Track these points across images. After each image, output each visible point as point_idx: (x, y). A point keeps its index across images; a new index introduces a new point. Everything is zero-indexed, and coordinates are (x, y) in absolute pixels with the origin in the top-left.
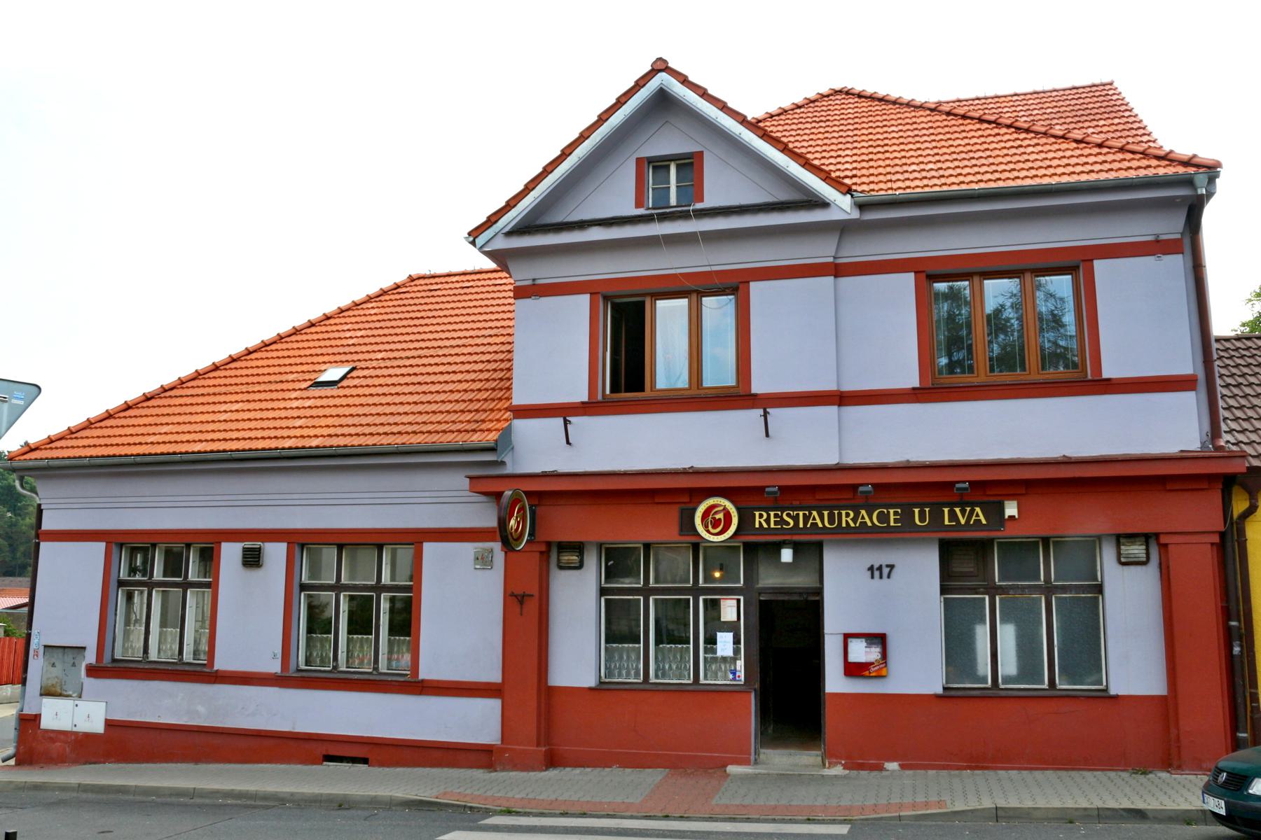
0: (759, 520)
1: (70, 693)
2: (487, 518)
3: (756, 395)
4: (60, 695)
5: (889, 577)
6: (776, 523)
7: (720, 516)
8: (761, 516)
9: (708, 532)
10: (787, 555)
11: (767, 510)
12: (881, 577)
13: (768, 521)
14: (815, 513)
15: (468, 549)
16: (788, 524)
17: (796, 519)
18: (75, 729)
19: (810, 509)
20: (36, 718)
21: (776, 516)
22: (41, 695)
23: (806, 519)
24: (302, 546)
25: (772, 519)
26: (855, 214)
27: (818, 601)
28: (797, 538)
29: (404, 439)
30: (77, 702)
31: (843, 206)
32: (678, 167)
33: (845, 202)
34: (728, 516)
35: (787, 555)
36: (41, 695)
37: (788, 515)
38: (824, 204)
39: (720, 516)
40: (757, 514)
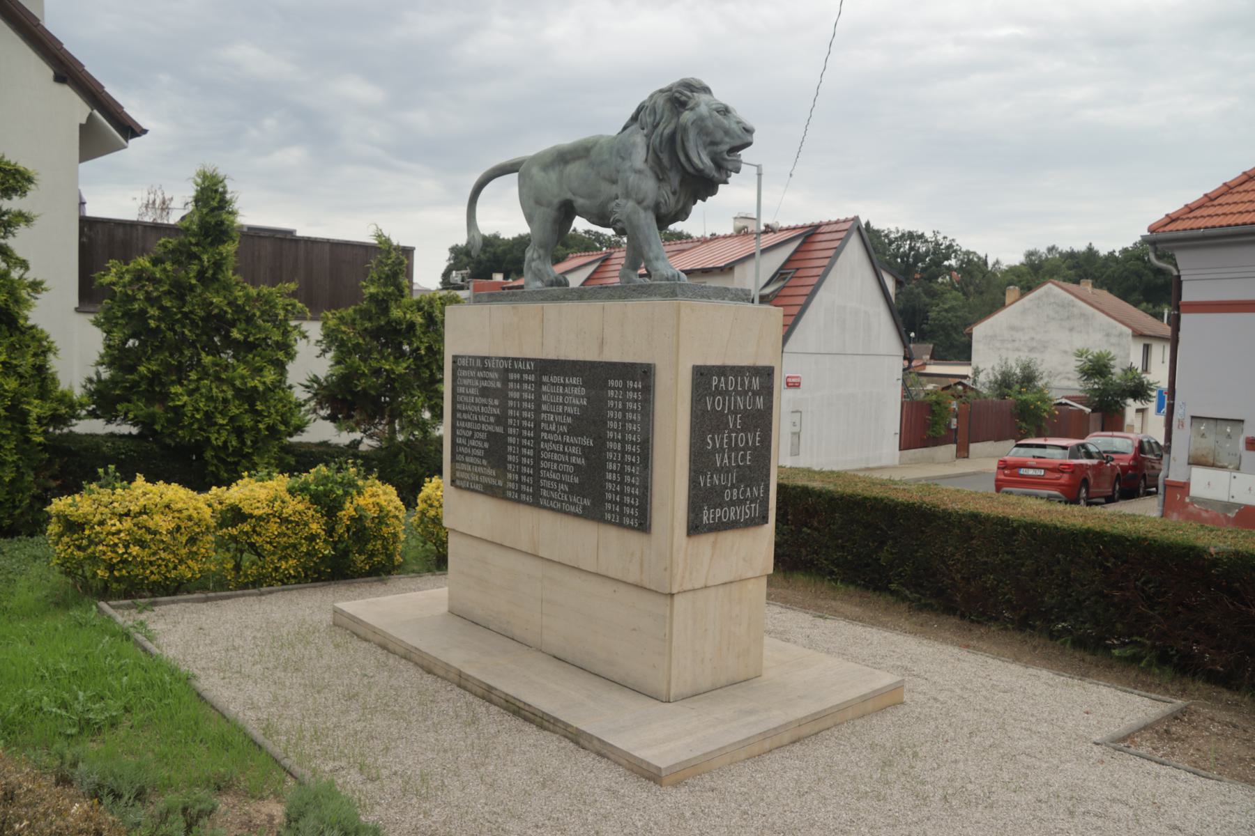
1: (1226, 464)
4: (1213, 466)
18: (1232, 500)
20: (1184, 487)
22: (1189, 464)
30: (1234, 474)
36: (1189, 464)
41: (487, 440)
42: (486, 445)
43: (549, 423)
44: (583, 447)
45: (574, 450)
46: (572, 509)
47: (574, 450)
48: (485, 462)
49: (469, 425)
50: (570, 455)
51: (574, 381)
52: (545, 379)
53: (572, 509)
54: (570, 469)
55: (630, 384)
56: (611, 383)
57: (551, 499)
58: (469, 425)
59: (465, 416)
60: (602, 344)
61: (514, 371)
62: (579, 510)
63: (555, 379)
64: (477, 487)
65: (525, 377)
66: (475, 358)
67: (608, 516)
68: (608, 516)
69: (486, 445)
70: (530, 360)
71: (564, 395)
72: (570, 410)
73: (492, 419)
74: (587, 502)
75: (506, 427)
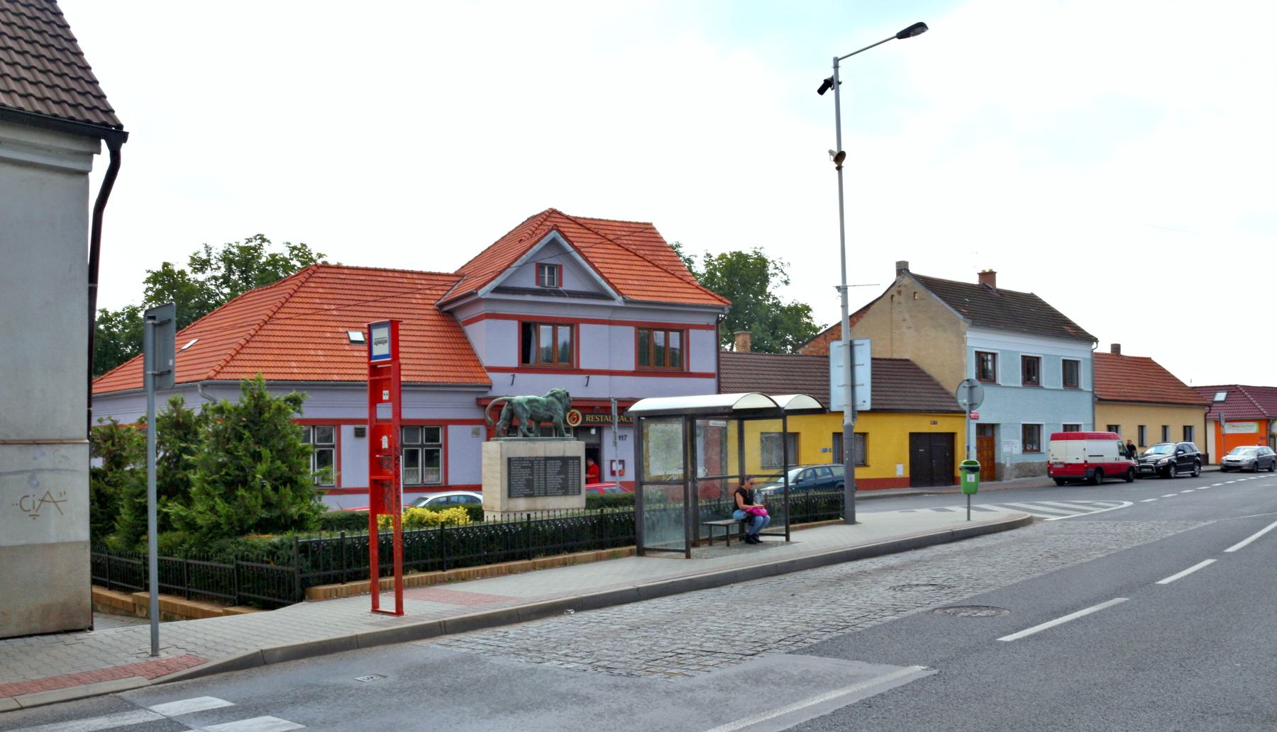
0: (588, 418)
2: (475, 414)
10: (593, 432)
11: (590, 414)
15: (468, 429)
24: (314, 427)
26: (623, 305)
31: (619, 301)
33: (620, 298)
34: (578, 417)
35: (593, 432)
38: (612, 299)
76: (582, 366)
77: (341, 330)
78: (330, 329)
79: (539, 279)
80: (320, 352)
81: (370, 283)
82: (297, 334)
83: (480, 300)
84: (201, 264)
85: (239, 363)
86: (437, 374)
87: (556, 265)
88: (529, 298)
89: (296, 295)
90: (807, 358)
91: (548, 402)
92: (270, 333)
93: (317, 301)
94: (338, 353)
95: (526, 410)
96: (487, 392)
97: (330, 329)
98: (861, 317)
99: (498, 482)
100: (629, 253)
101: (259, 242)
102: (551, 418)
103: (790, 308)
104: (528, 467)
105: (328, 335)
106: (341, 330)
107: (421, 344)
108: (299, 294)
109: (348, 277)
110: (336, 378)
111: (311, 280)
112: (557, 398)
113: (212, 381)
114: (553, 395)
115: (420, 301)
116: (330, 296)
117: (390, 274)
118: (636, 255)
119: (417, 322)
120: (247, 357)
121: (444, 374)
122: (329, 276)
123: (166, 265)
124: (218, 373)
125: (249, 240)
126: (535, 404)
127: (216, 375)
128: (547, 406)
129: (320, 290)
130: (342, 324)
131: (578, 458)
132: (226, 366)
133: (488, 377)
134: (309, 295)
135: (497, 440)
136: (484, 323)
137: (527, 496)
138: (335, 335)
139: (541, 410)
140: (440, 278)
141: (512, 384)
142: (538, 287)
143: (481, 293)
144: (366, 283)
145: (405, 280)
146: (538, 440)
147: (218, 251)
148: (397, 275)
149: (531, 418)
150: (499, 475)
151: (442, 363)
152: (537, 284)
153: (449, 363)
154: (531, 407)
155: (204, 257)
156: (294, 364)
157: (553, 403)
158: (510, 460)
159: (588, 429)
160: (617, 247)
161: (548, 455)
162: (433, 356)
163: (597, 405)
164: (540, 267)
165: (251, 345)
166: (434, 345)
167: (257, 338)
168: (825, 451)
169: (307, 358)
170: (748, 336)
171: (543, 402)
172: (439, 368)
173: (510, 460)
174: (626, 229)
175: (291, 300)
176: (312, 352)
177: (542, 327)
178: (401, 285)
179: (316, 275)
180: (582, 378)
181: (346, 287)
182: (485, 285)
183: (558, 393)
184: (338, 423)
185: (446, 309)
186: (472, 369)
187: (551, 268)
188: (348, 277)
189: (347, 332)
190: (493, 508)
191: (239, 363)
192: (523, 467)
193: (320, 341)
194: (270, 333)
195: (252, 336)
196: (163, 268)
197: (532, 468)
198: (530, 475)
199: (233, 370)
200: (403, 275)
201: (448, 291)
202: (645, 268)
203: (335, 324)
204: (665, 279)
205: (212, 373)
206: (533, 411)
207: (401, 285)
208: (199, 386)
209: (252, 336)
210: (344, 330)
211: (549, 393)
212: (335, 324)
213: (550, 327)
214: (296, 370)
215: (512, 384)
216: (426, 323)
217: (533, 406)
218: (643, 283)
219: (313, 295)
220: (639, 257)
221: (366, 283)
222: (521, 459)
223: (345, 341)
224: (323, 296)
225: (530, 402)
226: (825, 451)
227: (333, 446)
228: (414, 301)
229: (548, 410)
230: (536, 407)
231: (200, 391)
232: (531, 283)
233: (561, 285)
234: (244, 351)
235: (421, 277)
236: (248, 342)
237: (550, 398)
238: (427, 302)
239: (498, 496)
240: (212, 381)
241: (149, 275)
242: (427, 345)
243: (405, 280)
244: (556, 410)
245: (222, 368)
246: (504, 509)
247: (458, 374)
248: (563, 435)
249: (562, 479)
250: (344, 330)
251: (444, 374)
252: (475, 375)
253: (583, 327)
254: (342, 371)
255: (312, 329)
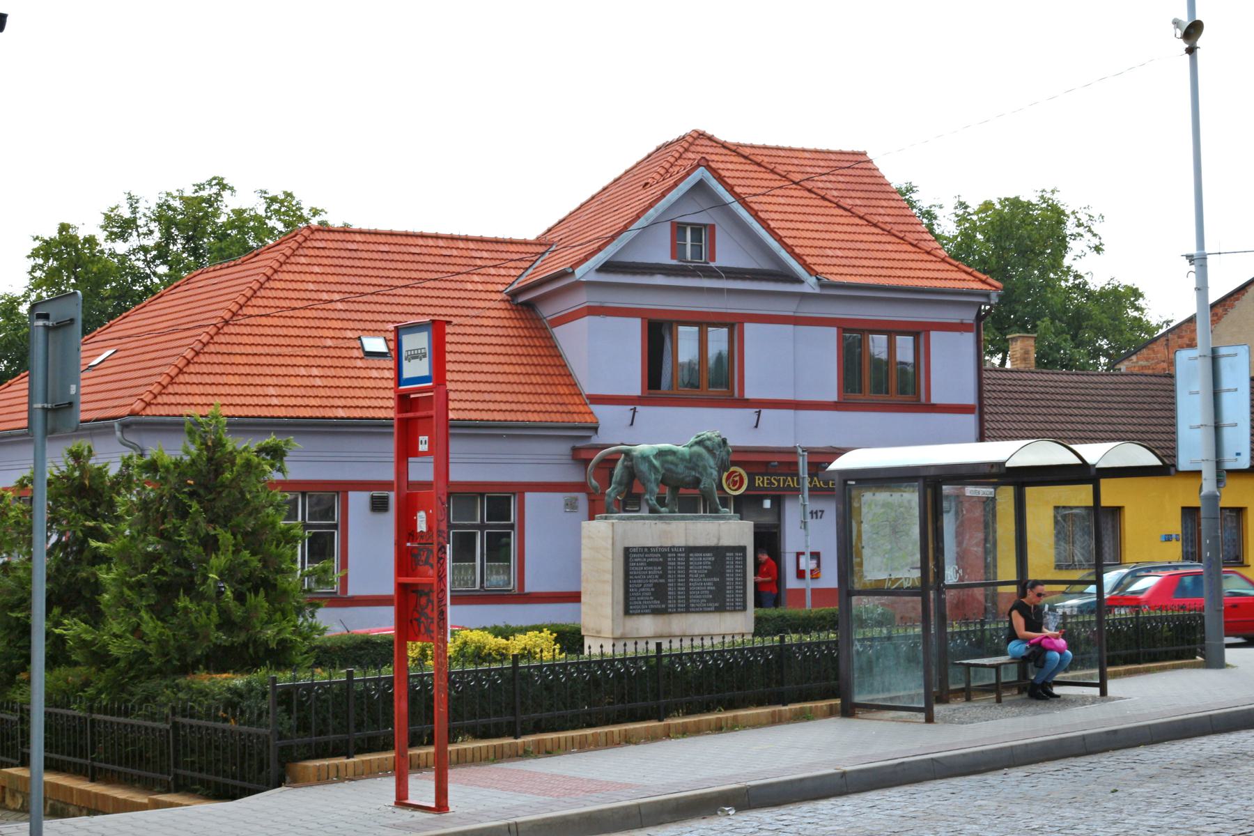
0: (758, 482)
2: (572, 475)
3: (748, 399)
5: (821, 517)
6: (767, 484)
7: (737, 478)
8: (759, 479)
9: (730, 488)
10: (767, 504)
11: (763, 475)
12: (817, 518)
13: (763, 482)
14: (789, 478)
15: (559, 498)
16: (774, 484)
17: (779, 481)
19: (787, 475)
21: (768, 479)
23: (784, 481)
24: (304, 494)
25: (765, 481)
26: (817, 290)
27: (776, 533)
28: (773, 493)
29: (520, 417)
32: (692, 229)
33: (812, 280)
35: (767, 504)
37: (775, 479)
38: (799, 281)
39: (737, 478)
40: (757, 477)
41: (654, 587)
42: (653, 589)
43: (694, 574)
44: (714, 582)
45: (709, 584)
46: (709, 609)
47: (709, 584)
48: (652, 598)
49: (640, 581)
50: (707, 586)
51: (708, 555)
52: (691, 555)
53: (709, 609)
54: (708, 592)
55: (737, 554)
56: (728, 554)
57: (697, 607)
58: (640, 581)
59: (636, 577)
60: (719, 539)
61: (671, 552)
62: (713, 609)
63: (697, 555)
64: (647, 611)
65: (679, 555)
66: (644, 548)
67: (728, 608)
68: (728, 608)
69: (653, 589)
70: (682, 547)
71: (702, 561)
72: (706, 567)
73: (657, 577)
74: (717, 605)
75: (666, 579)
76: (749, 394)
77: (349, 334)
78: (331, 333)
79: (677, 250)
80: (315, 371)
81: (397, 257)
82: (276, 341)
83: (579, 285)
84: (121, 227)
85: (183, 389)
86: (508, 407)
87: (705, 226)
88: (659, 280)
89: (276, 276)
90: (1135, 379)
91: (692, 455)
92: (234, 339)
93: (311, 286)
94: (344, 373)
95: (654, 467)
96: (589, 437)
97: (331, 333)
98: (1232, 307)
99: (609, 588)
100: (826, 203)
101: (215, 189)
102: (697, 482)
103: (1104, 294)
104: (657, 564)
105: (329, 343)
106: (349, 334)
107: (480, 358)
108: (280, 276)
109: (362, 247)
110: (341, 413)
111: (301, 252)
112: (706, 448)
113: (137, 418)
114: (700, 443)
115: (480, 287)
116: (331, 279)
117: (430, 242)
118: (839, 206)
119: (476, 321)
120: (194, 379)
121: (519, 407)
122: (330, 245)
123: (64, 228)
124: (148, 404)
125: (200, 187)
126: (670, 458)
127: (144, 409)
128: (690, 460)
129: (316, 269)
130: (351, 325)
131: (743, 549)
132: (160, 394)
133: (592, 413)
134: (298, 277)
135: (606, 518)
136: (586, 321)
137: (656, 612)
138: (340, 343)
139: (681, 469)
140: (512, 248)
141: (632, 424)
142: (675, 262)
143: (579, 273)
144: (391, 256)
145: (455, 252)
146: (674, 519)
147: (149, 203)
148: (441, 243)
149: (663, 482)
150: (609, 577)
151: (516, 388)
152: (673, 257)
153: (527, 389)
154: (663, 463)
155: (127, 214)
156: (271, 391)
157: (699, 456)
158: (627, 551)
159: (760, 499)
160: (806, 194)
161: (691, 543)
162: (501, 378)
163: (775, 459)
164: (678, 229)
165: (202, 358)
166: (502, 359)
167: (212, 348)
168: (1168, 538)
169: (293, 381)
170: (1032, 342)
171: (683, 454)
172: (509, 398)
173: (627, 551)
174: (822, 163)
175: (267, 285)
176: (303, 371)
177: (681, 329)
178: (448, 260)
179: (309, 244)
180: (750, 413)
181: (357, 263)
182: (586, 259)
183: (709, 439)
184: (343, 488)
185: (522, 299)
186: (566, 400)
187: (697, 230)
188: (362, 247)
189: (359, 338)
190: (598, 632)
191: (183, 389)
192: (649, 564)
193: (315, 352)
194: (234, 339)
195: (205, 345)
196: (60, 232)
197: (664, 565)
198: (661, 577)
199: (172, 399)
200: (451, 244)
201: (527, 269)
202: (854, 229)
203: (339, 324)
204: (889, 247)
205: (138, 406)
206: (668, 470)
207: (448, 260)
208: (116, 425)
209: (205, 345)
210: (356, 334)
211: (693, 440)
212: (339, 324)
213: (696, 329)
214: (275, 401)
215: (632, 424)
216: (491, 322)
217: (667, 462)
218: (850, 254)
219: (303, 277)
220: (845, 209)
221: (391, 256)
222: (645, 551)
223: (356, 353)
224: (320, 278)
225: (661, 454)
226: (1168, 538)
227: (335, 526)
228: (469, 286)
229: (693, 469)
230: (672, 463)
231: (118, 434)
232: (663, 256)
233: (713, 259)
234: (192, 368)
235: (482, 246)
236: (197, 354)
237: (696, 448)
238: (490, 287)
239: (608, 611)
240: (137, 418)
241: (37, 244)
242: (491, 359)
243: (455, 252)
244: (705, 468)
245: (155, 397)
246: (618, 634)
247: (542, 408)
248: (717, 511)
249: (715, 584)
250: (356, 334)
251: (519, 407)
252: (571, 408)
253: (749, 328)
254: (350, 402)
255: (302, 332)
